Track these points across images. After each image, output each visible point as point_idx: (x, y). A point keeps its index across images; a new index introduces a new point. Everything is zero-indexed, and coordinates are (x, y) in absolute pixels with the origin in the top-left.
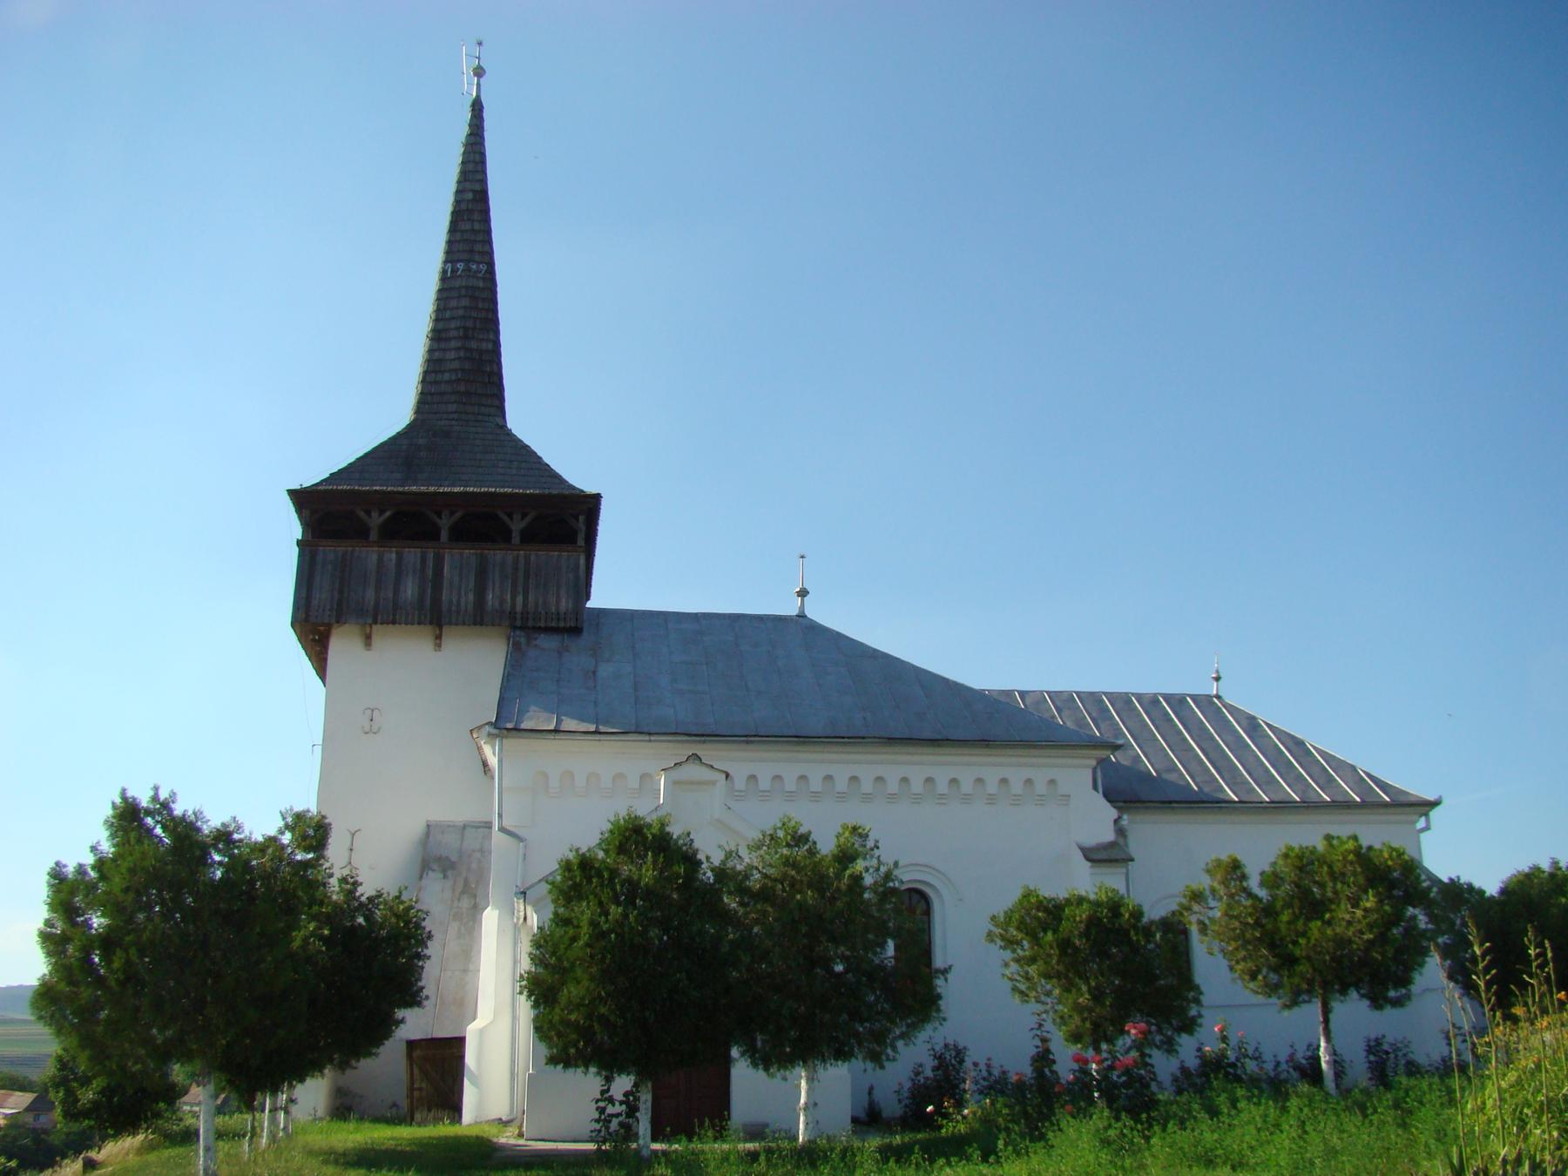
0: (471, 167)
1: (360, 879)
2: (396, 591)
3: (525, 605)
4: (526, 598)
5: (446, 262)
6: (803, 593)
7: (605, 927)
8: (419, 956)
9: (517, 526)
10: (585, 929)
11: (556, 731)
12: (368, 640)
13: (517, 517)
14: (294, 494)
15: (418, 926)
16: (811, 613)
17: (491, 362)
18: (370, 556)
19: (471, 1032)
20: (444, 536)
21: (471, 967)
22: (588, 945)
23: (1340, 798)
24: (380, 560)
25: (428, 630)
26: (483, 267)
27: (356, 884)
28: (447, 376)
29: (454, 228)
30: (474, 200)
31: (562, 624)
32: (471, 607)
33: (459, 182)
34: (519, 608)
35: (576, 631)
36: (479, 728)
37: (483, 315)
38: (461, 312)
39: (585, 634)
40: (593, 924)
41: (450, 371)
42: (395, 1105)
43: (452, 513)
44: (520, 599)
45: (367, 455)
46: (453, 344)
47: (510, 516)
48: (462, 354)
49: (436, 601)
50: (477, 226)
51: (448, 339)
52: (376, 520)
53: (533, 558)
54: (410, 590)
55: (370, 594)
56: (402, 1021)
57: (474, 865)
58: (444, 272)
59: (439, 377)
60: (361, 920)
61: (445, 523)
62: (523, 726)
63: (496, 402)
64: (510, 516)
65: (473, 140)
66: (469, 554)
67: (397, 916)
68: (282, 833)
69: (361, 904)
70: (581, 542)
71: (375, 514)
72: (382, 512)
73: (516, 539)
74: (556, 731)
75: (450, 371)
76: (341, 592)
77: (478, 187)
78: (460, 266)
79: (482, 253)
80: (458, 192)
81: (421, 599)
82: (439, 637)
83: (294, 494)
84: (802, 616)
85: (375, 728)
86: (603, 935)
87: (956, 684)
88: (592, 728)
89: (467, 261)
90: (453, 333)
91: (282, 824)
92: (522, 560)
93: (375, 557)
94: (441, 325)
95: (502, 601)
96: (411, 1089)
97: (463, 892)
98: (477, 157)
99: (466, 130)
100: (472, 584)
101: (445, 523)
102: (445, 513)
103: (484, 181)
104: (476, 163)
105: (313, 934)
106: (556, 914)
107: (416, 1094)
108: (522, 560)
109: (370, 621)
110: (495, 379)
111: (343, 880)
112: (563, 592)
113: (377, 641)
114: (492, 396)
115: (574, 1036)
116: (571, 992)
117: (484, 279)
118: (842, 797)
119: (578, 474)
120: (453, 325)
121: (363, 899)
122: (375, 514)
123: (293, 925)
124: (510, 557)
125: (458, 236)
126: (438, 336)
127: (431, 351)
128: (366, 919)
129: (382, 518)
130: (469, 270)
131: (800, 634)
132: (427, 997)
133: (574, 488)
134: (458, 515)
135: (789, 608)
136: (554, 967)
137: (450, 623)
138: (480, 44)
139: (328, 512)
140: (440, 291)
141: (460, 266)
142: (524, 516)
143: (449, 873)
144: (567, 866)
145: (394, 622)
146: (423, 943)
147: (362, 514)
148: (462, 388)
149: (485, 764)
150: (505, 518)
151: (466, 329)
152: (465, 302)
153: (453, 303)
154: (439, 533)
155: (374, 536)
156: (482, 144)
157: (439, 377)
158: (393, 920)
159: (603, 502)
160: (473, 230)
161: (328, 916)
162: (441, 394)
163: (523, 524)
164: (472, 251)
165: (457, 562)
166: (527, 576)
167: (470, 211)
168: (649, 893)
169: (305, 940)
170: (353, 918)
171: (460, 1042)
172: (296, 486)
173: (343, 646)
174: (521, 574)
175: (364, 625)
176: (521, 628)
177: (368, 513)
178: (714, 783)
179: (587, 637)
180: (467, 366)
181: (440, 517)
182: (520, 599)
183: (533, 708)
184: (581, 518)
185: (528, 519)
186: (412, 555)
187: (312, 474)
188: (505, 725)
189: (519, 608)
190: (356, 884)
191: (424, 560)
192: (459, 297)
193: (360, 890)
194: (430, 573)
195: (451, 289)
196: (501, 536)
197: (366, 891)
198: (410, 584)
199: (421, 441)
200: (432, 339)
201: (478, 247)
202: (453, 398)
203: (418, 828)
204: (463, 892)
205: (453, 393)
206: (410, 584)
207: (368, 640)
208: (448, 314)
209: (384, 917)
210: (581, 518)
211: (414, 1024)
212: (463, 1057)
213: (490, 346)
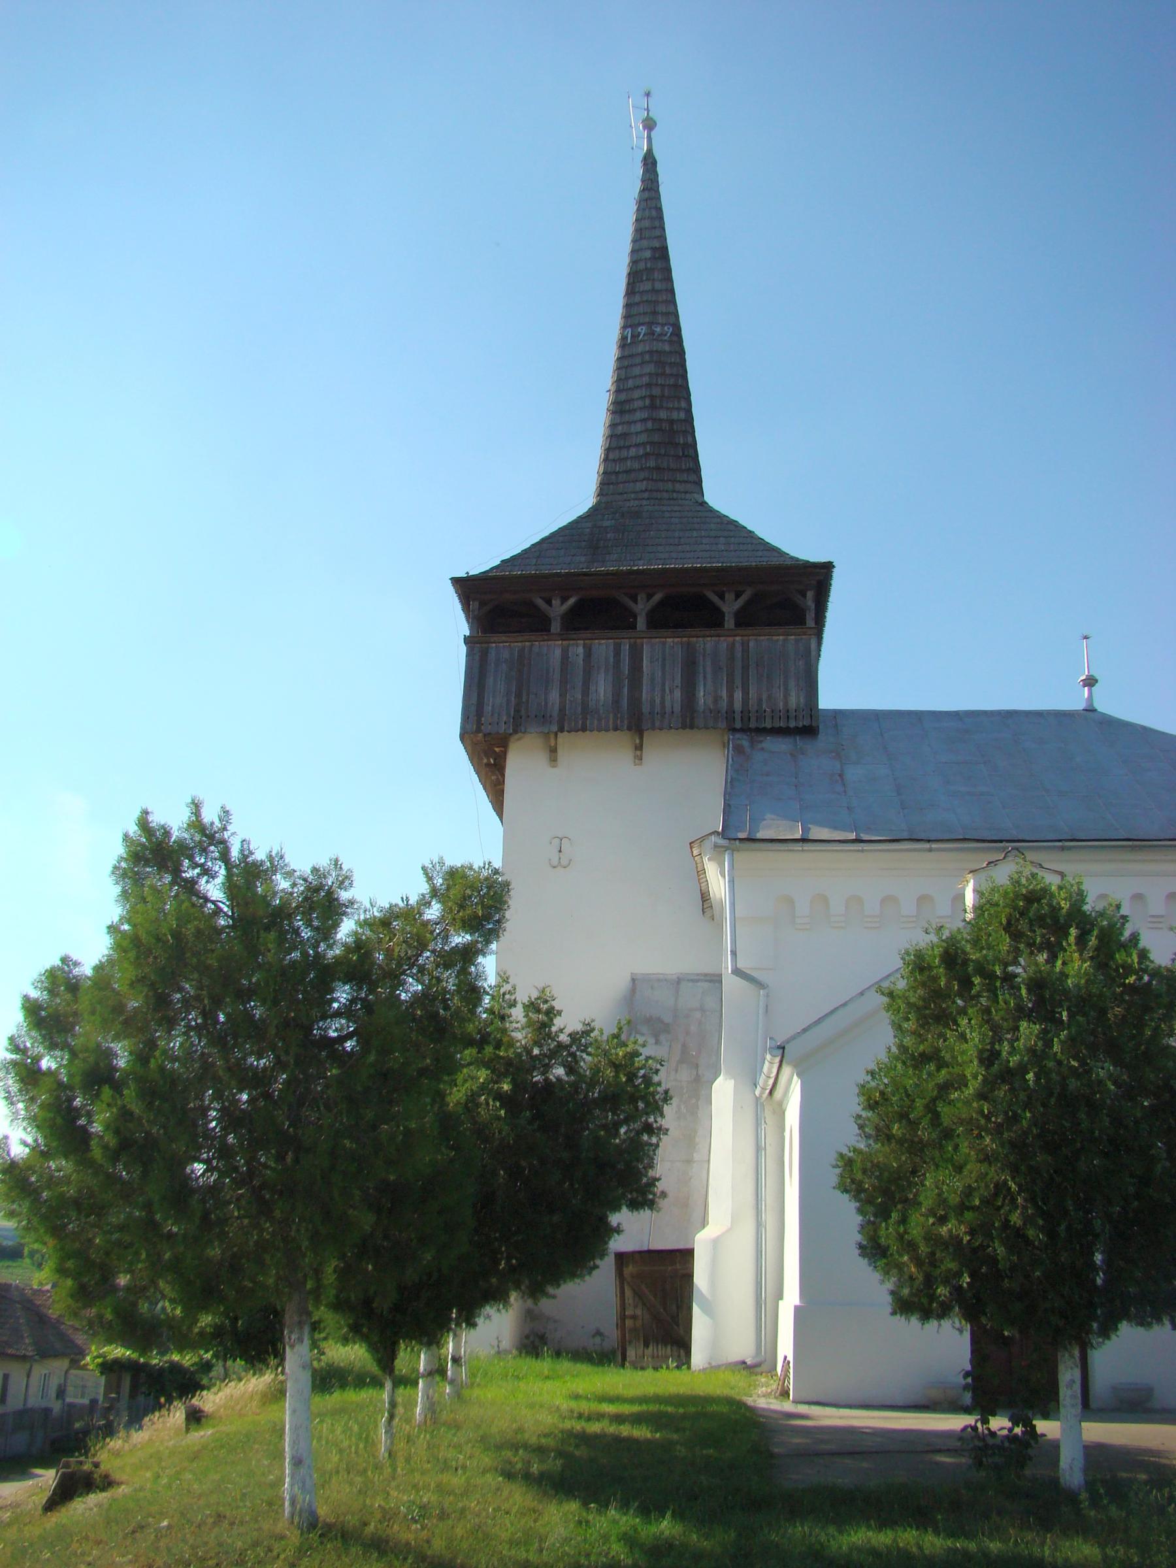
0: (646, 223)
1: (557, 1005)
2: (586, 691)
3: (745, 701)
4: (746, 692)
5: (624, 327)
7: (1014, 1060)
8: (649, 1129)
9: (730, 607)
10: (973, 1071)
11: (804, 840)
12: (553, 753)
13: (729, 596)
14: (457, 582)
15: (647, 1080)
16: (1101, 706)
17: (685, 432)
18: (551, 651)
19: (702, 1242)
20: (641, 623)
21: (696, 1156)
22: (982, 1096)
25: (624, 739)
26: (669, 330)
27: (551, 1013)
28: (633, 452)
29: (631, 291)
30: (653, 258)
31: (792, 724)
32: (677, 708)
33: (634, 241)
34: (738, 706)
35: (809, 731)
36: (702, 839)
37: (672, 381)
38: (646, 380)
39: (821, 736)
40: (989, 1058)
41: (637, 445)
42: (598, 1333)
43: (650, 596)
44: (738, 695)
45: (543, 540)
46: (639, 415)
47: (722, 597)
48: (649, 425)
49: (635, 702)
50: (658, 286)
52: (558, 609)
53: (751, 644)
54: (602, 689)
55: (554, 696)
56: (618, 1230)
57: (693, 1028)
58: (623, 338)
59: (624, 453)
60: (560, 1071)
62: (759, 835)
63: (693, 477)
64: (722, 597)
65: (646, 195)
66: (672, 644)
67: (616, 1067)
68: (428, 904)
69: (560, 1046)
70: (810, 623)
72: (564, 599)
73: (729, 623)
74: (804, 840)
75: (637, 445)
76: (519, 695)
77: (656, 244)
78: (642, 330)
79: (667, 314)
80: (633, 252)
81: (616, 701)
82: (639, 747)
83: (457, 582)
84: (1090, 710)
85: (564, 862)
86: (1010, 1075)
88: (853, 836)
89: (650, 324)
90: (636, 404)
91: (425, 888)
92: (738, 648)
93: (558, 653)
94: (623, 397)
95: (717, 699)
96: (623, 1317)
97: (681, 1061)
98: (654, 213)
99: (638, 185)
100: (678, 681)
101: (642, 608)
102: (641, 597)
103: (663, 238)
104: (651, 218)
105: (483, 1088)
106: (903, 1048)
107: (629, 1323)
108: (738, 648)
109: (555, 728)
110: (691, 452)
111: (532, 1006)
112: (792, 683)
114: (689, 470)
115: (952, 1265)
116: (938, 1184)
117: (671, 342)
120: (637, 394)
121: (564, 1038)
122: (556, 602)
123: (447, 1068)
124: (724, 643)
125: (637, 298)
126: (620, 408)
127: (613, 426)
128: (570, 1070)
131: (1085, 733)
132: (664, 1195)
133: (797, 560)
134: (657, 597)
135: (1075, 700)
136: (901, 1142)
137: (653, 729)
138: (648, 95)
139: (500, 605)
140: (619, 359)
141: (642, 330)
142: (738, 596)
143: (662, 1038)
144: (919, 965)
145: (584, 729)
146: (656, 1108)
147: (540, 602)
148: (652, 463)
149: (705, 897)
150: (715, 599)
151: (652, 397)
153: (637, 371)
154: (636, 620)
155: (556, 627)
156: (657, 197)
157: (624, 453)
158: (610, 1073)
159: (836, 574)
160: (654, 291)
161: (509, 1063)
164: (654, 313)
165: (660, 654)
166: (745, 668)
167: (649, 271)
168: (1083, 1003)
169: (472, 1098)
170: (547, 1068)
171: (687, 1255)
172: (461, 574)
173: (523, 763)
174: (738, 664)
175: (546, 735)
176: (742, 730)
177: (549, 602)
179: (824, 739)
180: (656, 438)
181: (636, 602)
182: (738, 695)
183: (768, 816)
184: (810, 594)
186: (603, 648)
187: (481, 560)
188: (736, 836)
189: (738, 706)
190: (551, 1013)
191: (617, 653)
193: (558, 1022)
195: (631, 356)
196: (711, 619)
197: (567, 1023)
198: (602, 683)
199: (606, 523)
200: (613, 413)
201: (661, 308)
202: (642, 475)
204: (681, 1061)
205: (642, 469)
206: (602, 683)
207: (553, 753)
208: (630, 383)
209: (596, 1070)
210: (810, 594)
211: (633, 1230)
212: (690, 1276)
213: (682, 415)
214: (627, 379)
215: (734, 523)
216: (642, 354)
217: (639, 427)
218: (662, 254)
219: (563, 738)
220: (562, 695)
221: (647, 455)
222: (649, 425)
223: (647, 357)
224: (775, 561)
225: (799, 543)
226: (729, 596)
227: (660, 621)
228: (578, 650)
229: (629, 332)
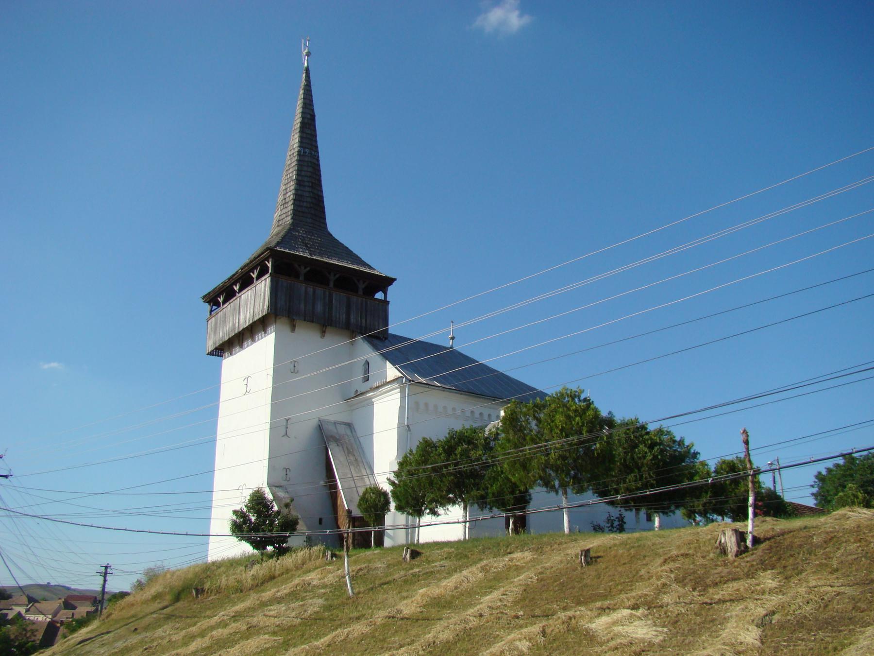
12: (293, 328)
18: (302, 288)
20: (332, 284)
28: (305, 204)
34: (364, 325)
38: (309, 174)
51: (305, 186)
54: (319, 308)
55: (302, 306)
61: (332, 278)
71: (303, 268)
73: (361, 292)
89: (311, 149)
93: (304, 289)
94: (300, 178)
119: (381, 269)
142: (364, 282)
145: (312, 321)
147: (296, 266)
163: (363, 286)
164: (311, 145)
165: (338, 297)
177: (299, 266)
182: (364, 321)
186: (320, 291)
189: (364, 325)
207: (293, 328)
208: (303, 173)
218: (313, 117)
220: (305, 306)
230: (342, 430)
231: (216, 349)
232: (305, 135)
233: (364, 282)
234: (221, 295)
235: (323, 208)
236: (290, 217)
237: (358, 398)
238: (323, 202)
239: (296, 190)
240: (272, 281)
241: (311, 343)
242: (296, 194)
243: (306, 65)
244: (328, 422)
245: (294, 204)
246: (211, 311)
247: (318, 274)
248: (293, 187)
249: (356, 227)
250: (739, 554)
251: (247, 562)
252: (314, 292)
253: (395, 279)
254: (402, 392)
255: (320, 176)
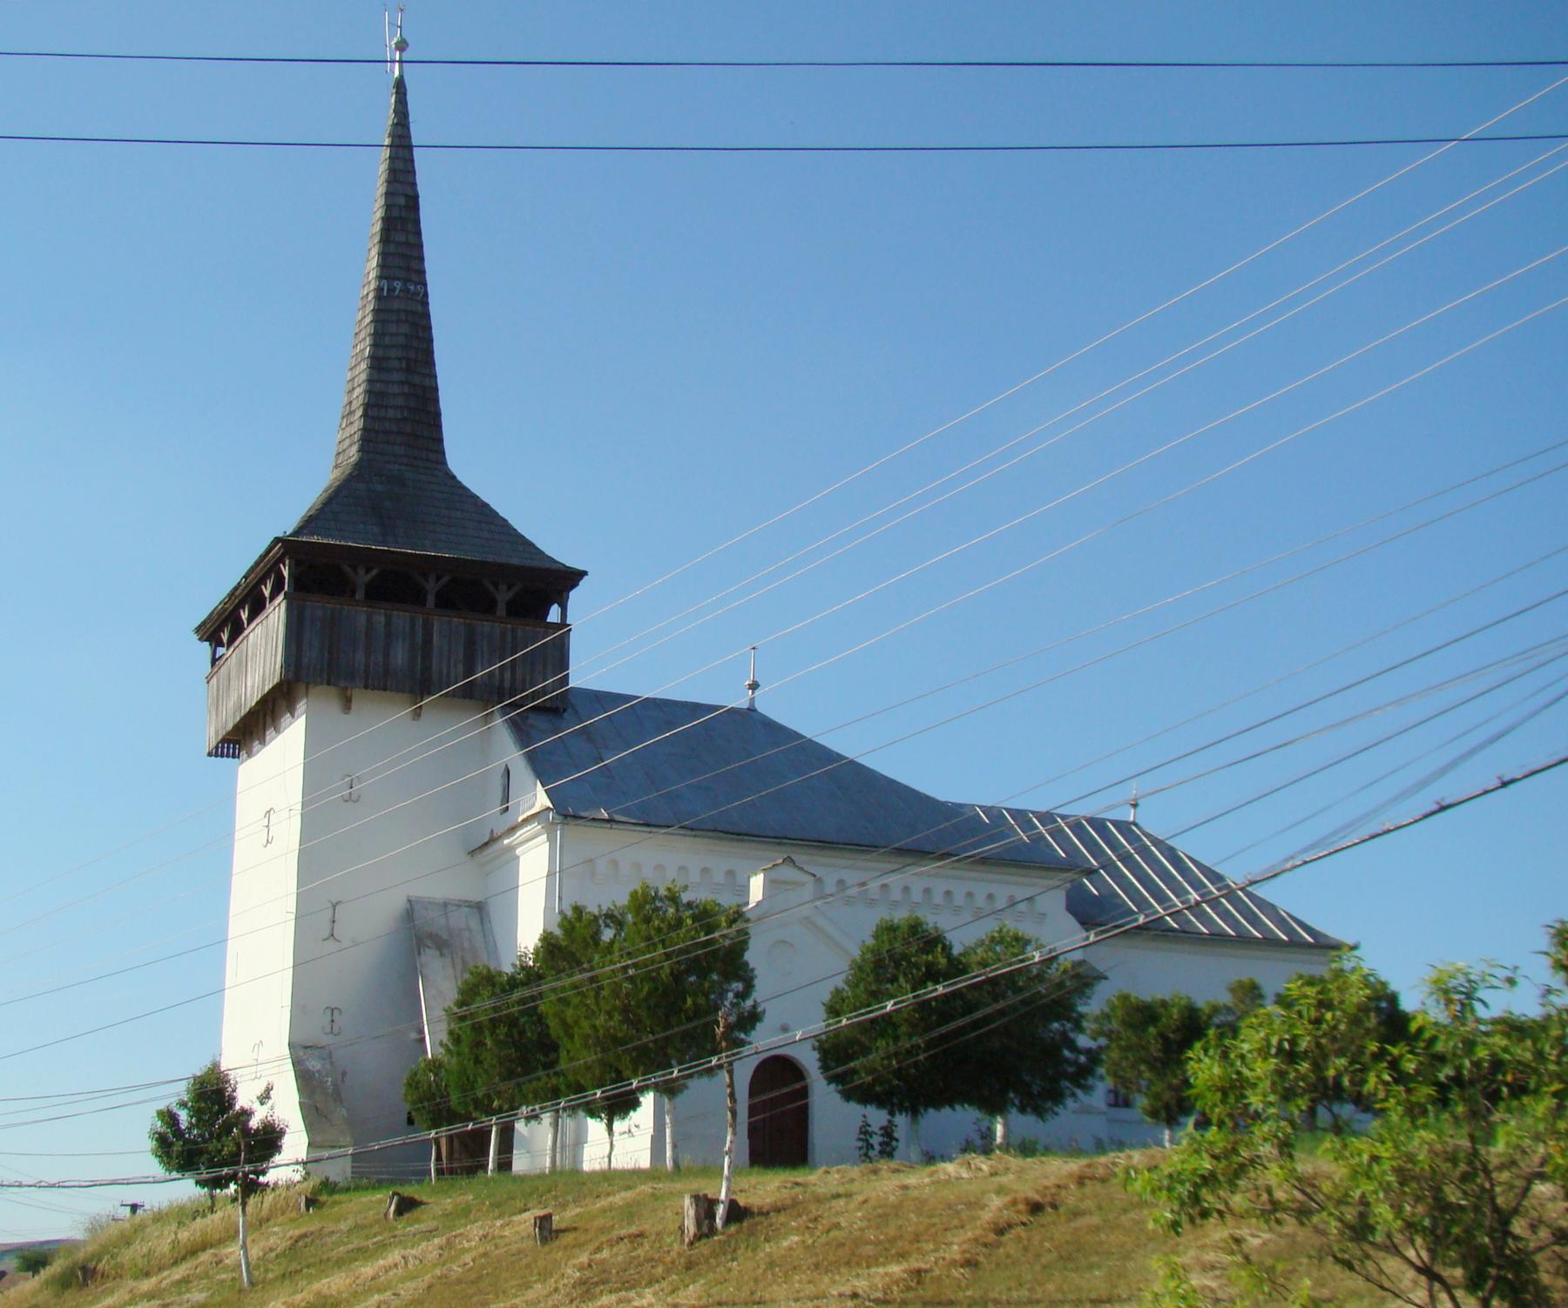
2: (387, 654)
6: (754, 686)
9: (503, 596)
12: (347, 704)
13: (503, 587)
18: (360, 616)
23: (1216, 931)
24: (369, 620)
28: (391, 413)
30: (407, 207)
38: (401, 340)
41: (396, 407)
43: (438, 578)
47: (496, 585)
48: (406, 389)
52: (363, 578)
53: (520, 633)
54: (400, 655)
55: (360, 657)
59: (382, 413)
61: (432, 587)
64: (496, 585)
71: (361, 571)
72: (368, 571)
73: (501, 610)
75: (396, 407)
78: (398, 285)
80: (388, 194)
84: (752, 709)
87: (928, 797)
89: (406, 281)
90: (395, 364)
92: (509, 635)
94: (380, 353)
101: (432, 587)
113: (354, 705)
118: (872, 903)
119: (558, 547)
120: (393, 353)
122: (361, 571)
129: (369, 577)
130: (408, 290)
131: (747, 726)
134: (446, 579)
135: (741, 702)
142: (509, 588)
143: (445, 951)
145: (385, 689)
147: (347, 569)
148: (408, 429)
150: (491, 588)
151: (408, 359)
152: (405, 329)
153: (393, 328)
157: (382, 413)
160: (407, 244)
162: (385, 432)
163: (510, 595)
164: (409, 269)
165: (446, 630)
178: (803, 884)
185: (516, 589)
186: (401, 618)
191: (413, 626)
192: (399, 321)
194: (419, 638)
195: (390, 311)
203: (393, 903)
207: (347, 704)
208: (387, 340)
214: (384, 334)
215: (486, 505)
216: (399, 311)
217: (395, 389)
219: (357, 693)
221: (404, 419)
222: (406, 389)
223: (403, 317)
224: (547, 565)
225: (563, 552)
226: (503, 587)
227: (446, 602)
228: (380, 619)
229: (385, 283)
230: (458, 919)
231: (223, 741)
232: (392, 249)
233: (509, 588)
234: (223, 628)
235: (438, 414)
236: (355, 448)
237: (487, 849)
238: (437, 401)
239: (370, 381)
240: (288, 610)
241: (386, 731)
242: (369, 392)
243: (397, 73)
244: (429, 904)
245: (365, 415)
246: (214, 661)
247: (396, 583)
248: (363, 377)
249: (503, 458)
250: (699, 1237)
251: (184, 1214)
252: (388, 623)
253: (584, 573)
254: (551, 840)
255: (431, 340)
